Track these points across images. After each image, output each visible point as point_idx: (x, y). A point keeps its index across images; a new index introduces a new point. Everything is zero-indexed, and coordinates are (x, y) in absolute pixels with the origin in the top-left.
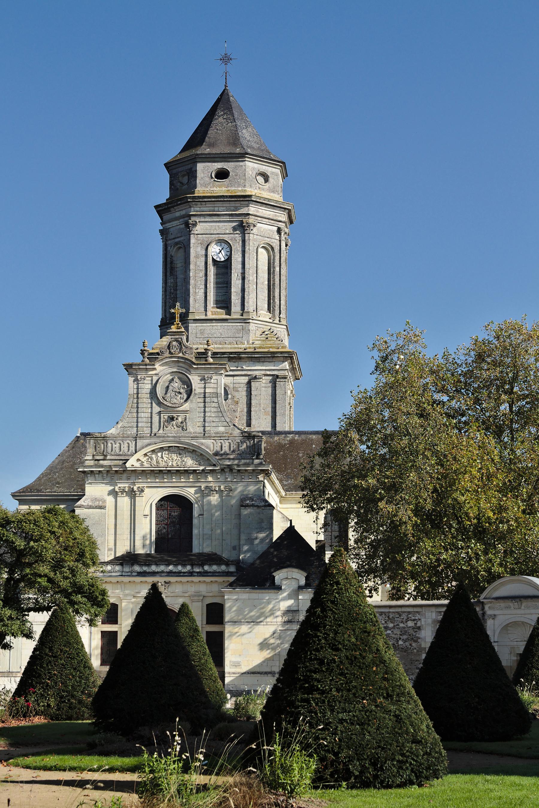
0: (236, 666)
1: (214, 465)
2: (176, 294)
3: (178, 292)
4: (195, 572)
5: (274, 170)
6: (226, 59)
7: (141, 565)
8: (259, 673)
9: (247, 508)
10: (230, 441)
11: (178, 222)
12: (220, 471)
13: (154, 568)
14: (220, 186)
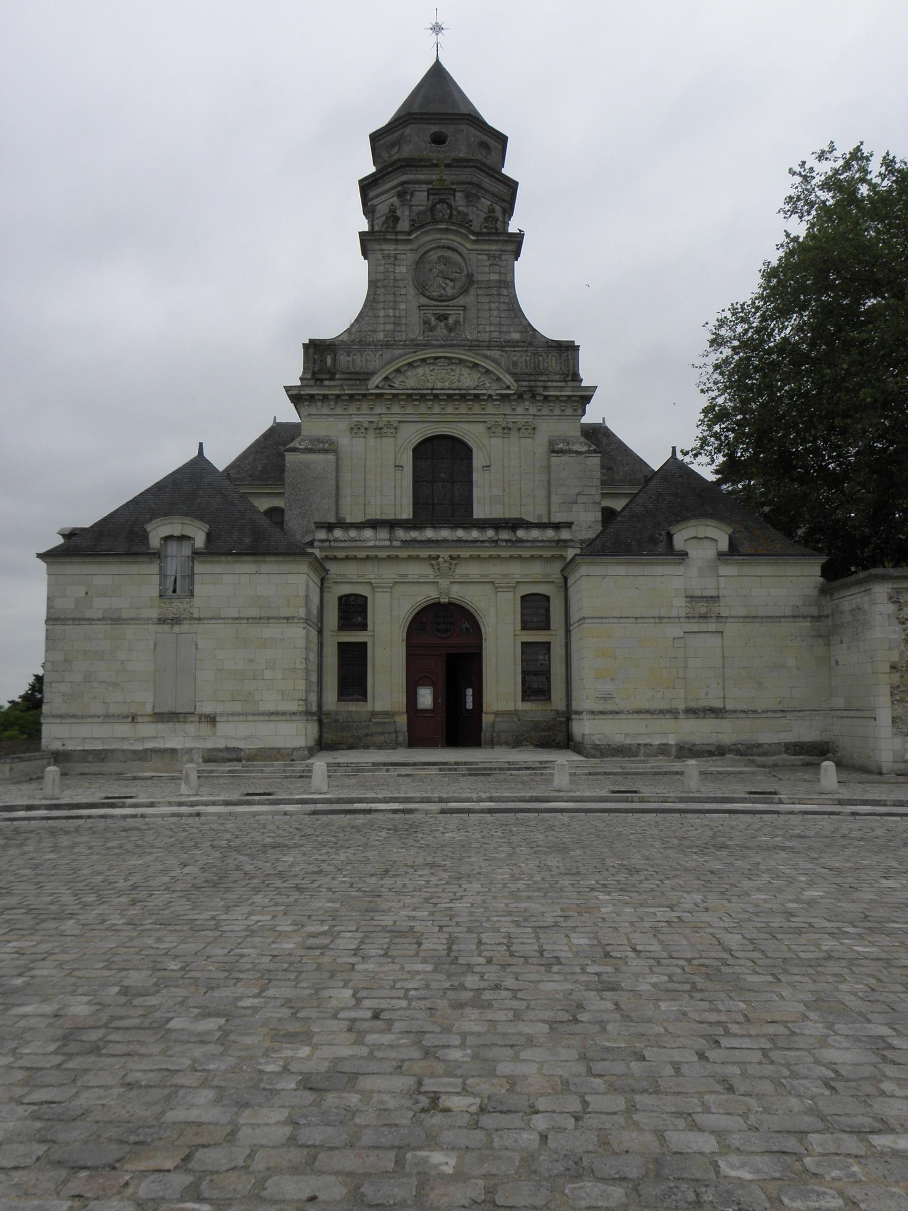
0: (605, 699)
1: (508, 388)
4: (502, 540)
5: (496, 144)
8: (648, 712)
12: (516, 397)
13: (429, 534)
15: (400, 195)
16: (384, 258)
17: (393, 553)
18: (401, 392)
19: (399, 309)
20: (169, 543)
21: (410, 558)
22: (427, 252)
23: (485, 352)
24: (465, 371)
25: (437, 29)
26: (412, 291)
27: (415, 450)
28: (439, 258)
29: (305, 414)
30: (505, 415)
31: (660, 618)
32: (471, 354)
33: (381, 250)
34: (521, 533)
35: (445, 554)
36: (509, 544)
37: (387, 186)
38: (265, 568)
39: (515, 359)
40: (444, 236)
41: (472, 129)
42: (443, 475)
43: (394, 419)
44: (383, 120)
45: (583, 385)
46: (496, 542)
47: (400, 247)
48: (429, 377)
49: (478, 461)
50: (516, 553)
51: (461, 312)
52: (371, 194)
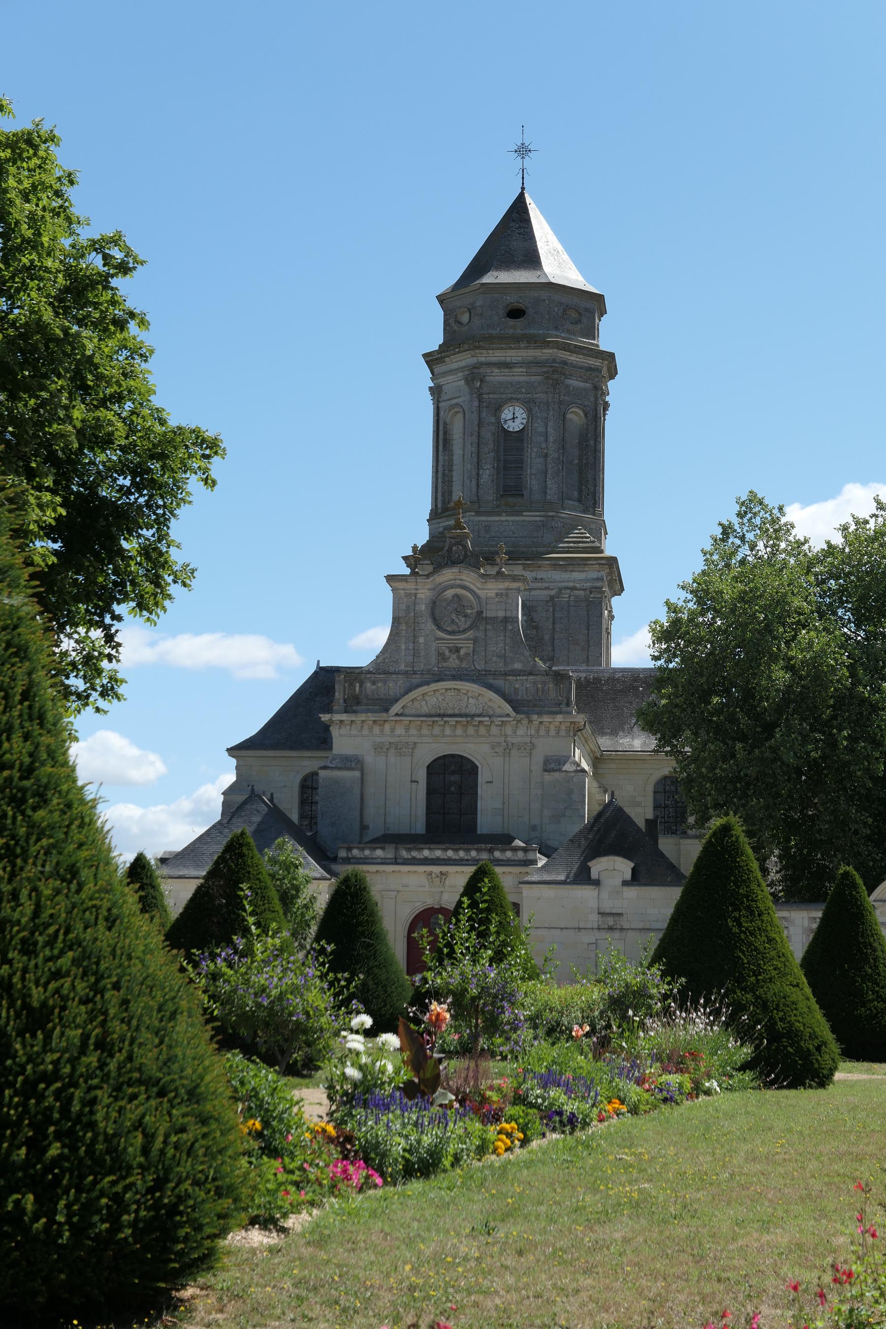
3: (454, 473)
7: (409, 850)
13: (426, 853)
25: (523, 151)
26: (430, 626)
31: (579, 929)
35: (436, 869)
49: (483, 777)
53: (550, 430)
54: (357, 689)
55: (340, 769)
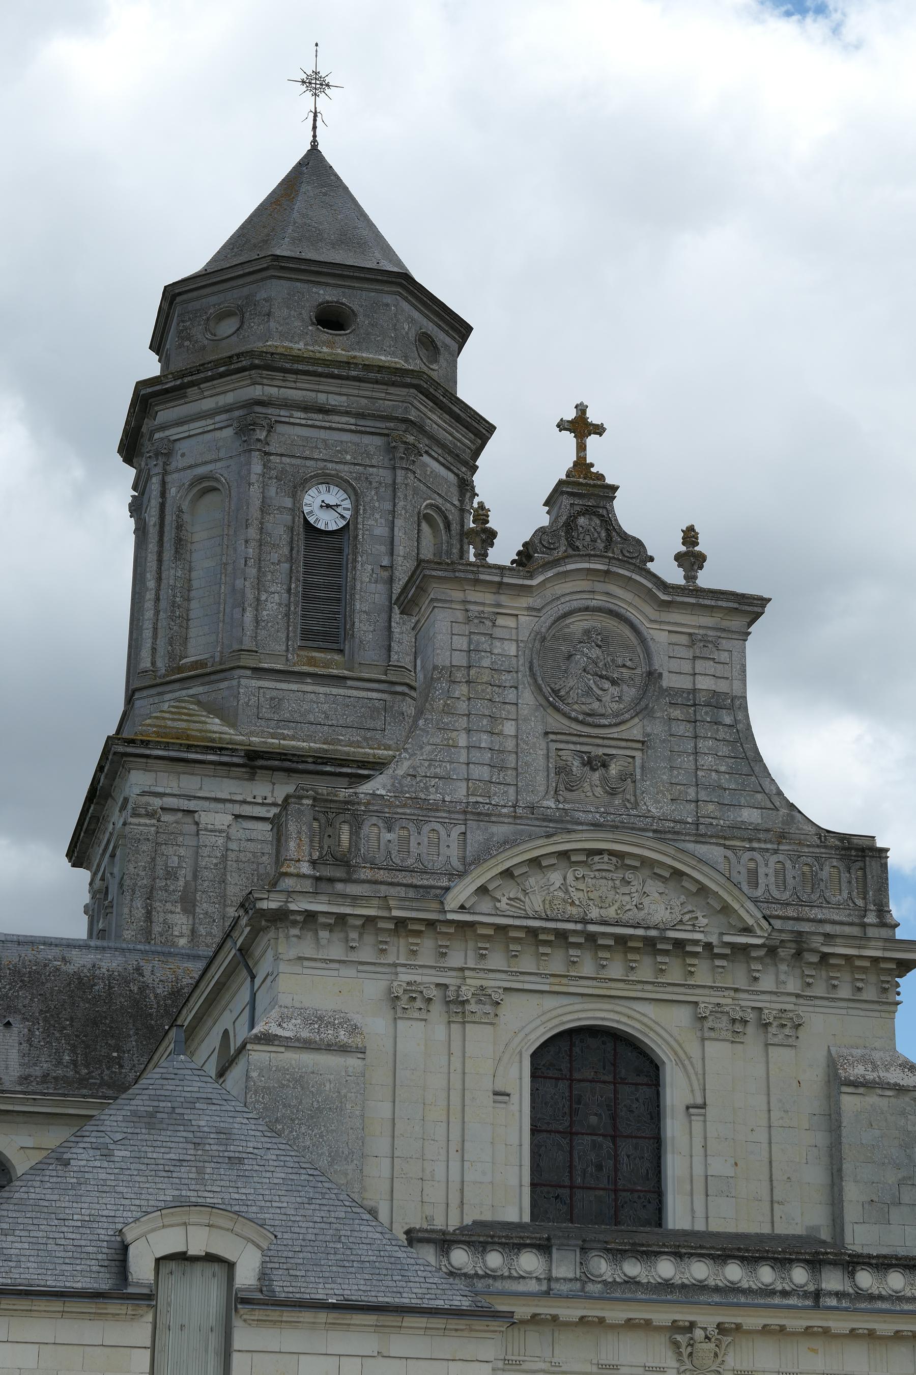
1: (747, 930)
2: (188, 610)
3: (194, 604)
4: (830, 1294)
5: (448, 340)
6: (316, 83)
7: (617, 1254)
9: (861, 1090)
10: (781, 858)
11: (210, 421)
12: (762, 952)
14: (331, 345)
15: (245, 429)
16: (468, 620)
17: (593, 1311)
18: (518, 922)
19: (500, 734)
20: (164, 1269)
21: (630, 1324)
22: (566, 615)
23: (690, 846)
24: (654, 887)
26: (528, 697)
27: (534, 1056)
28: (587, 632)
29: (293, 953)
30: (736, 990)
32: (672, 851)
33: (465, 602)
34: (865, 1279)
36: (844, 1304)
37: (208, 404)
38: (399, 1345)
39: (752, 865)
40: (599, 587)
41: (405, 305)
42: (593, 1120)
43: (492, 983)
44: (193, 255)
45: (900, 934)
46: (817, 1295)
47: (504, 599)
48: (576, 895)
49: (676, 1091)
50: (863, 1324)
51: (638, 754)
52: (164, 415)
53: (399, 534)
54: (345, 837)
55: (307, 1045)
